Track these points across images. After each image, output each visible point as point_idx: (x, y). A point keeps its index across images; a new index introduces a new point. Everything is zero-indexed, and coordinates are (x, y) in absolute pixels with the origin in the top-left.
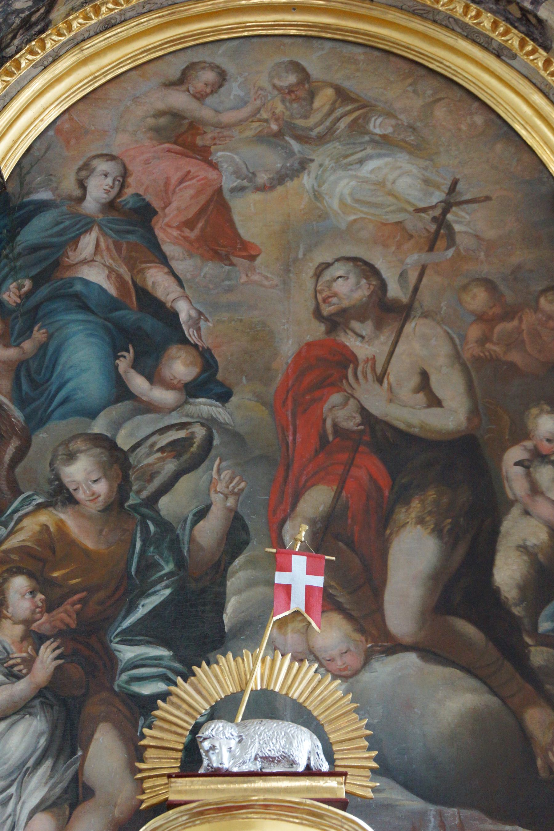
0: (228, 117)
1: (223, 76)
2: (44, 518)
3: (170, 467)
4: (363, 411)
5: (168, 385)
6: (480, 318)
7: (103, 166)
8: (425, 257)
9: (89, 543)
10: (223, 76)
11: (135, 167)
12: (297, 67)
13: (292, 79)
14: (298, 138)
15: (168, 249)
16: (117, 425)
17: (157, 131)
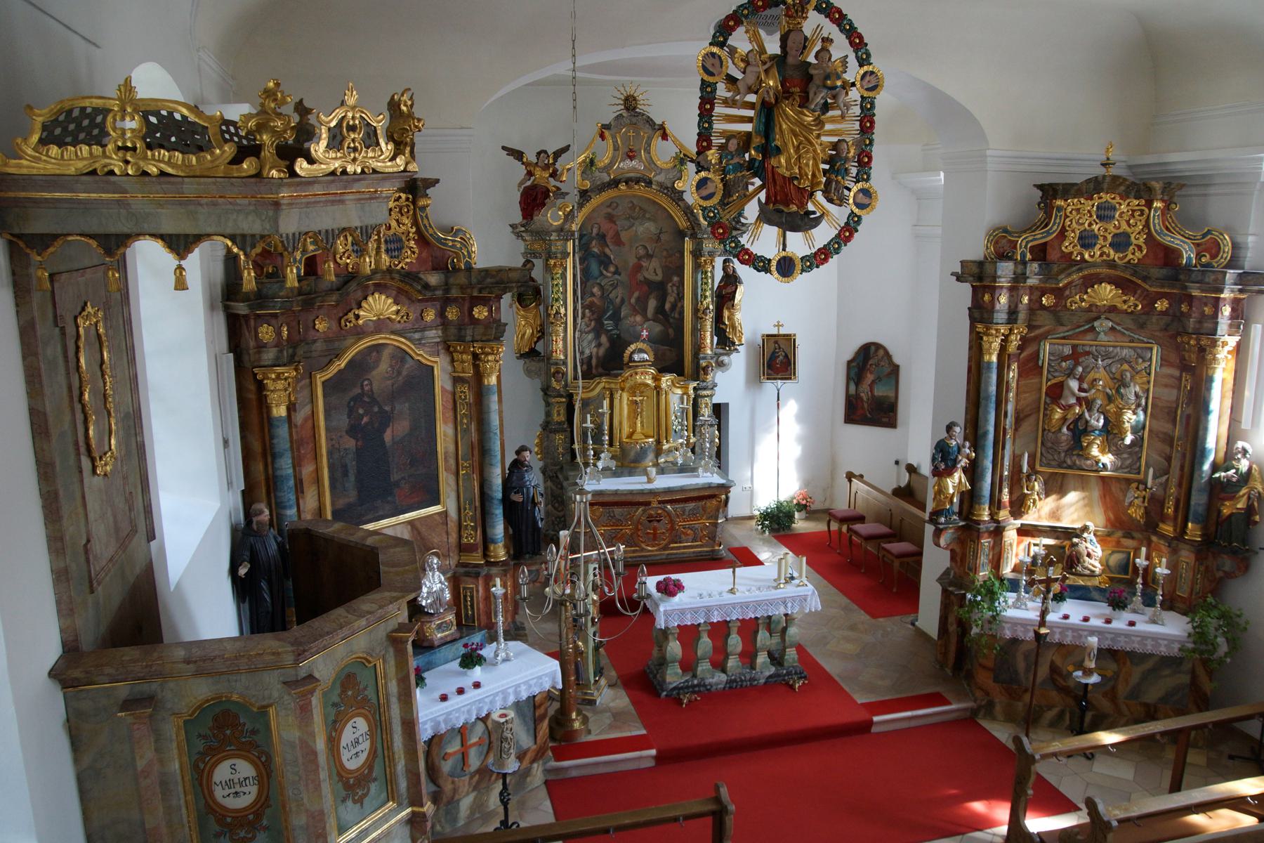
0: (619, 214)
1: (617, 204)
2: (590, 299)
3: (611, 289)
4: (645, 278)
5: (610, 272)
6: (665, 257)
7: (596, 226)
8: (655, 245)
9: (598, 303)
10: (617, 207)
11: (602, 226)
12: (632, 202)
13: (631, 205)
14: (633, 219)
15: (609, 244)
16: (601, 281)
17: (605, 217)
